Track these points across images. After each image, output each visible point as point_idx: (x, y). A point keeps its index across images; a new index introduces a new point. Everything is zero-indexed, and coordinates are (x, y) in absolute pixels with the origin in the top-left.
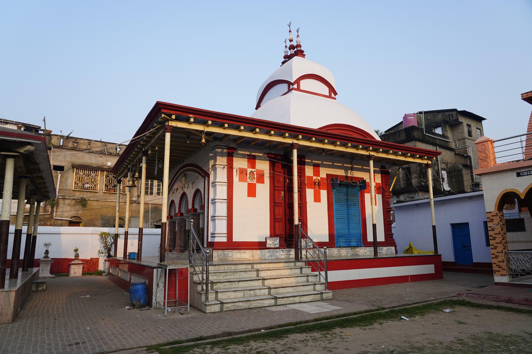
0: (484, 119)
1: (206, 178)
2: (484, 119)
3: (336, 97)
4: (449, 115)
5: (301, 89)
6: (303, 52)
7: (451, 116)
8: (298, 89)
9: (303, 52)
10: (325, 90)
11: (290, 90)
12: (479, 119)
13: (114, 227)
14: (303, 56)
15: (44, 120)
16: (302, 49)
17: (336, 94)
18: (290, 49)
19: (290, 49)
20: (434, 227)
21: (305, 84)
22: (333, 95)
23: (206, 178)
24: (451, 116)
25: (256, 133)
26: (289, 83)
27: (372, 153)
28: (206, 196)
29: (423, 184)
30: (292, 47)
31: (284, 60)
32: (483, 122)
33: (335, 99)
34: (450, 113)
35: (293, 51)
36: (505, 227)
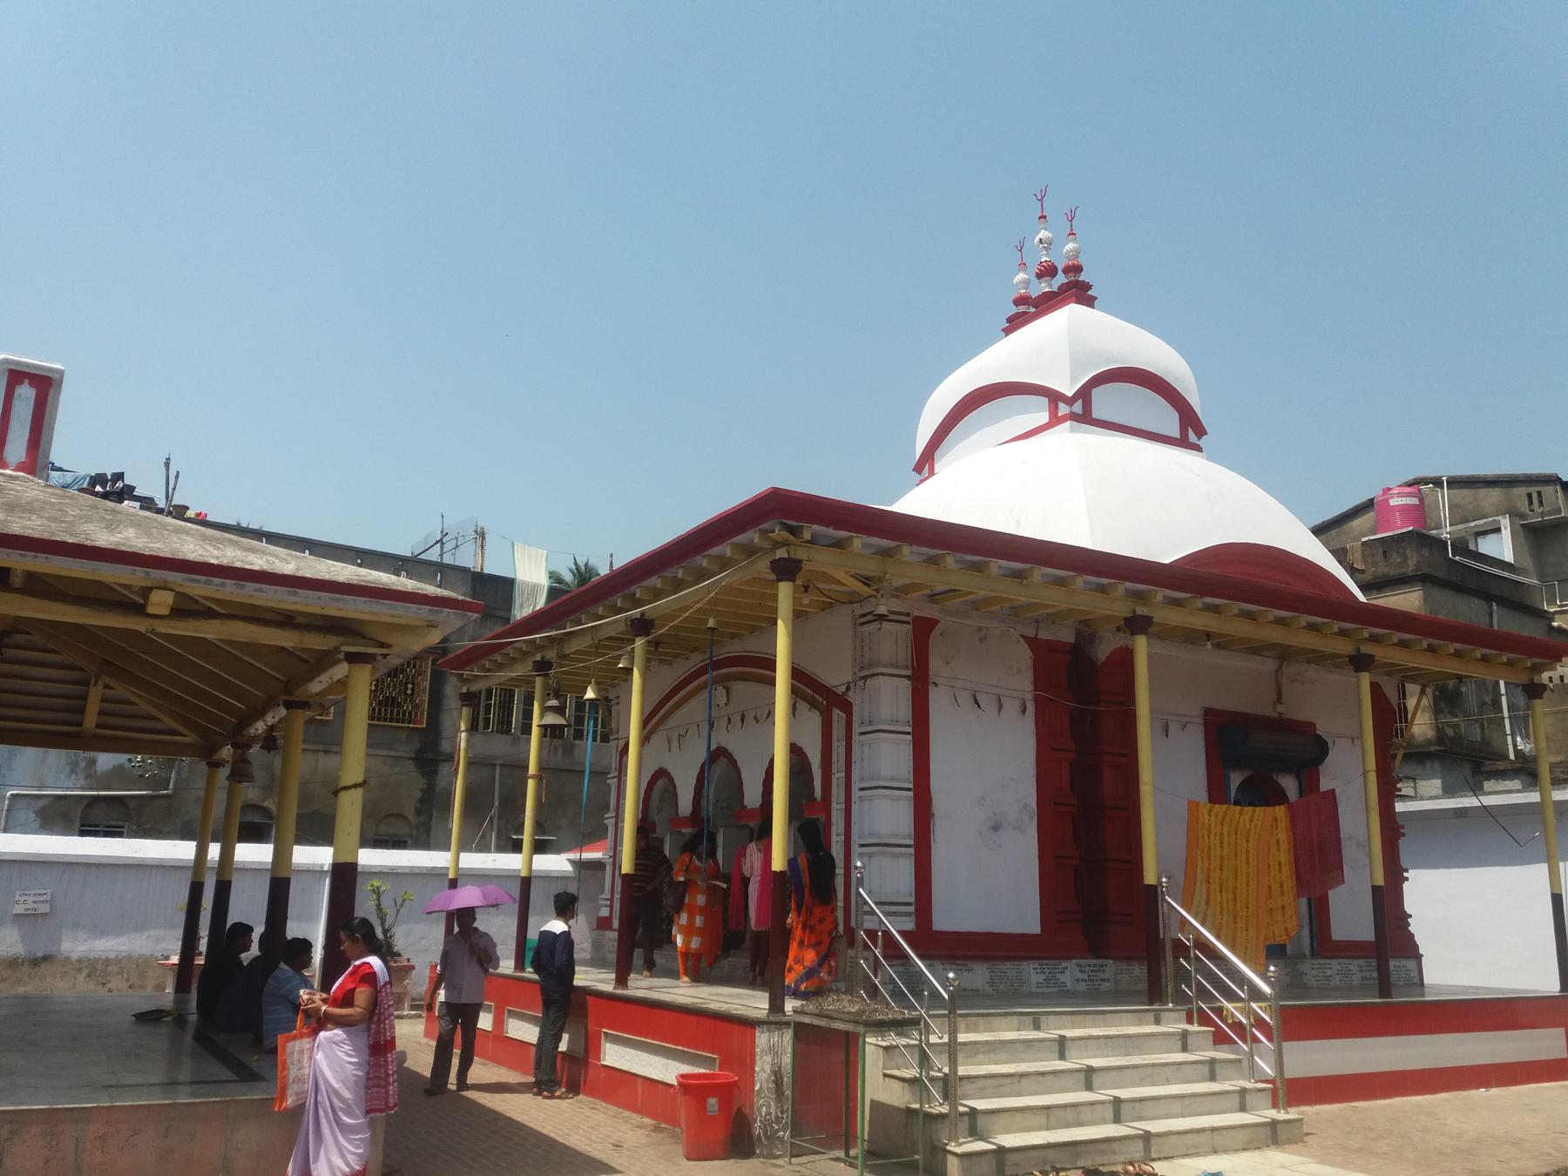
1: (837, 714)
4: (1530, 496)
5: (1096, 414)
6: (1089, 287)
7: (1535, 496)
8: (1086, 418)
9: (1089, 287)
10: (1170, 423)
11: (1055, 420)
14: (1090, 302)
16: (1083, 277)
17: (1201, 432)
18: (1039, 276)
19: (1039, 276)
21: (1106, 402)
22: (1192, 437)
23: (837, 714)
24: (1535, 496)
26: (1054, 397)
27: (1366, 649)
28: (838, 777)
29: (1450, 732)
30: (1048, 271)
31: (1014, 310)
33: (1198, 448)
34: (1533, 490)
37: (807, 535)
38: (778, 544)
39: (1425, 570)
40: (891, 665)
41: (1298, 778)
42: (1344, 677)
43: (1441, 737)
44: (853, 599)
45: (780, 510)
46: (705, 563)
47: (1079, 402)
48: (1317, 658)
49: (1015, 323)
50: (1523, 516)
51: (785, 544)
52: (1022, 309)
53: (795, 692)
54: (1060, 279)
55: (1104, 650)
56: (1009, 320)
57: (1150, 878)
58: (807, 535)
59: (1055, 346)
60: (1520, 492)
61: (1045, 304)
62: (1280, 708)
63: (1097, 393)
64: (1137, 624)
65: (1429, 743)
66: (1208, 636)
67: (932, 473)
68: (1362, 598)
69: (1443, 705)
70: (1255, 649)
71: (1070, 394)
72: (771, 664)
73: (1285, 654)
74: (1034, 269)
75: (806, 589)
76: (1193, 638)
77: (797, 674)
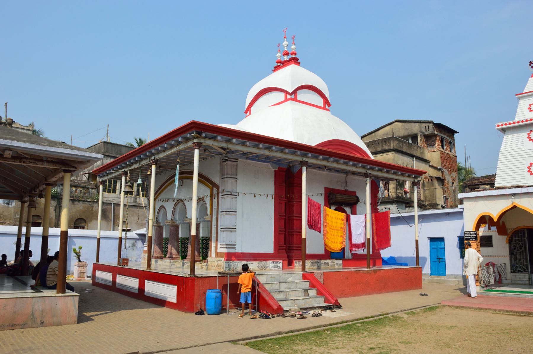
0: (457, 132)
2: (457, 132)
3: (330, 108)
6: (298, 59)
7: (427, 127)
8: (296, 100)
9: (298, 59)
10: (320, 101)
11: (286, 100)
12: (451, 132)
13: (97, 229)
14: (298, 64)
15: (6, 106)
16: (297, 56)
17: (329, 105)
20: (417, 241)
21: (303, 95)
22: (327, 107)
24: (427, 127)
25: (272, 151)
26: (286, 93)
27: (369, 172)
28: (215, 207)
29: (400, 195)
31: (276, 65)
32: (456, 135)
33: (328, 110)
34: (427, 125)
35: (286, 58)
36: (479, 244)
37: (204, 135)
38: (195, 138)
39: (395, 148)
40: (231, 175)
41: (351, 208)
42: (362, 178)
43: (398, 197)
44: (220, 154)
45: (196, 128)
46: (173, 143)
47: (293, 95)
48: (354, 173)
49: (277, 68)
50: (423, 133)
51: (197, 138)
52: (279, 64)
53: (199, 181)
54: (290, 56)
55: (296, 170)
56: (275, 68)
57: (303, 236)
58: (204, 135)
59: (288, 77)
60: (423, 125)
61: (283, 64)
62: (346, 188)
63: (299, 92)
64: (303, 163)
65: (394, 198)
66: (325, 166)
67: (250, 114)
68: (372, 157)
70: (338, 171)
71: (291, 92)
72: (192, 173)
73: (347, 172)
74: (283, 52)
75: (205, 150)
76: (320, 167)
77: (200, 175)
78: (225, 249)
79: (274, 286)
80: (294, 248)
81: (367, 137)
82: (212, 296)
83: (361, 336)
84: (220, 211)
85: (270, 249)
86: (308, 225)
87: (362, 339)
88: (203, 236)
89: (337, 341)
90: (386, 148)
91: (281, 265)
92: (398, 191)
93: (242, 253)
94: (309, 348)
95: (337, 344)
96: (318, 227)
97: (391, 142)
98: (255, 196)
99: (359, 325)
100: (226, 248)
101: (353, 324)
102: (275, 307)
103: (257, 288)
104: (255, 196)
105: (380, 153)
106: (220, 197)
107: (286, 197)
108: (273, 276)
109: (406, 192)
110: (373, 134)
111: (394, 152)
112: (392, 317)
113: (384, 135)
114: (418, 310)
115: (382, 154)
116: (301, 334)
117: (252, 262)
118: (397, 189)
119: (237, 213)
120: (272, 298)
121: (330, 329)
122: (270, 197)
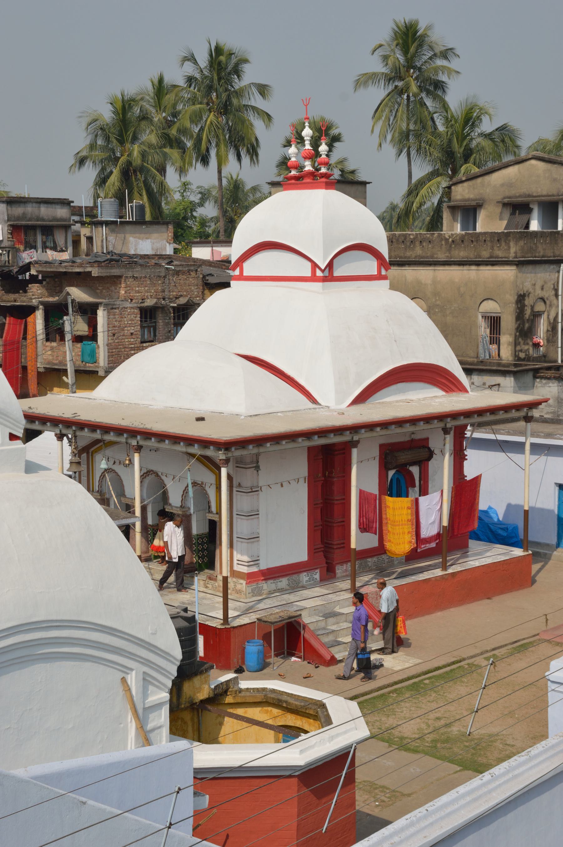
29: (522, 355)
69: (520, 340)
78: (246, 568)
79: (319, 624)
80: (335, 547)
81: (465, 184)
82: (253, 649)
83: (428, 699)
84: (235, 513)
85: (302, 555)
86: (360, 528)
87: (429, 704)
88: (198, 533)
89: (405, 709)
90: (500, 253)
91: (317, 576)
92: (518, 348)
93: (268, 569)
94: (378, 719)
95: (405, 712)
96: (372, 527)
97: (512, 244)
98: (282, 485)
99: (427, 682)
100: (248, 566)
101: (420, 681)
102: (328, 658)
103: (302, 632)
104: (282, 485)
105: (487, 265)
106: (235, 493)
107: (324, 475)
108: (316, 608)
109: (537, 345)
110: (479, 180)
111: (514, 268)
112: (467, 666)
113: (502, 185)
114: (503, 651)
115: (489, 268)
116: (366, 700)
117: (281, 580)
118: (516, 344)
119: (260, 516)
120: (316, 637)
121: (395, 691)
122: (302, 481)
